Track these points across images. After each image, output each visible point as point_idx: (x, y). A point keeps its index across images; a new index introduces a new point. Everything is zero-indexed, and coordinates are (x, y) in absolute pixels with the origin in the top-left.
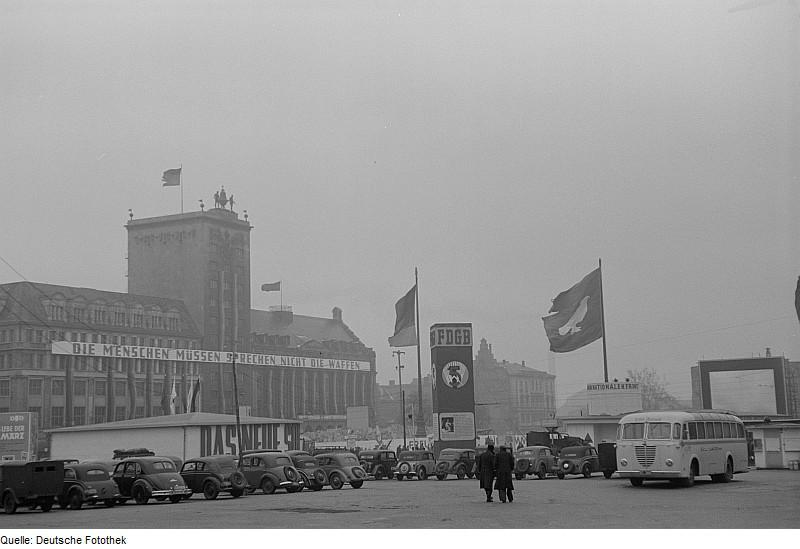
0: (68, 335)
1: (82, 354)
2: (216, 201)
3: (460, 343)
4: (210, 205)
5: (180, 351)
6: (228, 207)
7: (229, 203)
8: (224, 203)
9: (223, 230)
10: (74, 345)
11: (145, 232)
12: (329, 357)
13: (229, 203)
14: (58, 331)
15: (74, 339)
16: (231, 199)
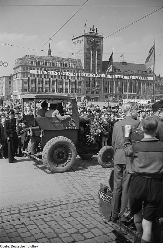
0: (36, 69)
1: (40, 73)
2: (91, 30)
3: (39, 73)
4: (88, 32)
5: (75, 73)
6: (95, 31)
7: (95, 31)
8: (93, 30)
9: (92, 38)
10: (38, 71)
11: (75, 40)
12: (135, 75)
13: (95, 31)
14: (33, 68)
15: (38, 69)
16: (96, 29)
